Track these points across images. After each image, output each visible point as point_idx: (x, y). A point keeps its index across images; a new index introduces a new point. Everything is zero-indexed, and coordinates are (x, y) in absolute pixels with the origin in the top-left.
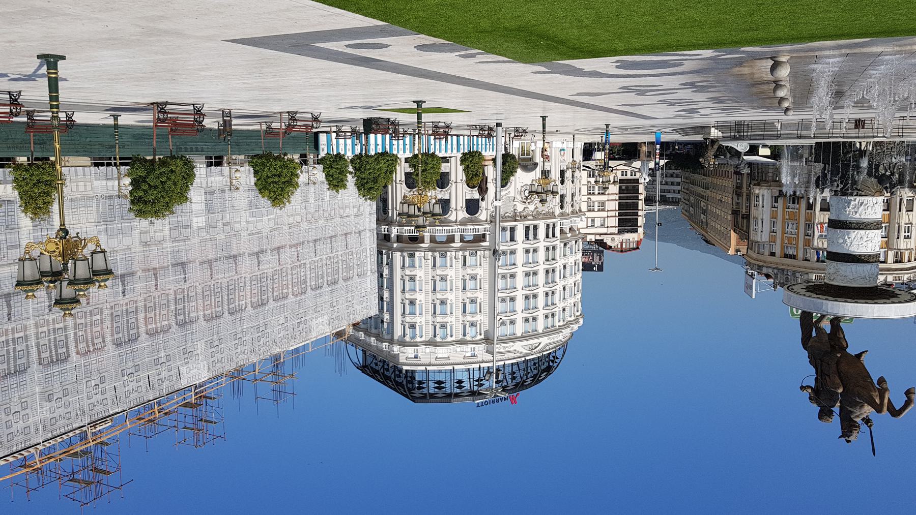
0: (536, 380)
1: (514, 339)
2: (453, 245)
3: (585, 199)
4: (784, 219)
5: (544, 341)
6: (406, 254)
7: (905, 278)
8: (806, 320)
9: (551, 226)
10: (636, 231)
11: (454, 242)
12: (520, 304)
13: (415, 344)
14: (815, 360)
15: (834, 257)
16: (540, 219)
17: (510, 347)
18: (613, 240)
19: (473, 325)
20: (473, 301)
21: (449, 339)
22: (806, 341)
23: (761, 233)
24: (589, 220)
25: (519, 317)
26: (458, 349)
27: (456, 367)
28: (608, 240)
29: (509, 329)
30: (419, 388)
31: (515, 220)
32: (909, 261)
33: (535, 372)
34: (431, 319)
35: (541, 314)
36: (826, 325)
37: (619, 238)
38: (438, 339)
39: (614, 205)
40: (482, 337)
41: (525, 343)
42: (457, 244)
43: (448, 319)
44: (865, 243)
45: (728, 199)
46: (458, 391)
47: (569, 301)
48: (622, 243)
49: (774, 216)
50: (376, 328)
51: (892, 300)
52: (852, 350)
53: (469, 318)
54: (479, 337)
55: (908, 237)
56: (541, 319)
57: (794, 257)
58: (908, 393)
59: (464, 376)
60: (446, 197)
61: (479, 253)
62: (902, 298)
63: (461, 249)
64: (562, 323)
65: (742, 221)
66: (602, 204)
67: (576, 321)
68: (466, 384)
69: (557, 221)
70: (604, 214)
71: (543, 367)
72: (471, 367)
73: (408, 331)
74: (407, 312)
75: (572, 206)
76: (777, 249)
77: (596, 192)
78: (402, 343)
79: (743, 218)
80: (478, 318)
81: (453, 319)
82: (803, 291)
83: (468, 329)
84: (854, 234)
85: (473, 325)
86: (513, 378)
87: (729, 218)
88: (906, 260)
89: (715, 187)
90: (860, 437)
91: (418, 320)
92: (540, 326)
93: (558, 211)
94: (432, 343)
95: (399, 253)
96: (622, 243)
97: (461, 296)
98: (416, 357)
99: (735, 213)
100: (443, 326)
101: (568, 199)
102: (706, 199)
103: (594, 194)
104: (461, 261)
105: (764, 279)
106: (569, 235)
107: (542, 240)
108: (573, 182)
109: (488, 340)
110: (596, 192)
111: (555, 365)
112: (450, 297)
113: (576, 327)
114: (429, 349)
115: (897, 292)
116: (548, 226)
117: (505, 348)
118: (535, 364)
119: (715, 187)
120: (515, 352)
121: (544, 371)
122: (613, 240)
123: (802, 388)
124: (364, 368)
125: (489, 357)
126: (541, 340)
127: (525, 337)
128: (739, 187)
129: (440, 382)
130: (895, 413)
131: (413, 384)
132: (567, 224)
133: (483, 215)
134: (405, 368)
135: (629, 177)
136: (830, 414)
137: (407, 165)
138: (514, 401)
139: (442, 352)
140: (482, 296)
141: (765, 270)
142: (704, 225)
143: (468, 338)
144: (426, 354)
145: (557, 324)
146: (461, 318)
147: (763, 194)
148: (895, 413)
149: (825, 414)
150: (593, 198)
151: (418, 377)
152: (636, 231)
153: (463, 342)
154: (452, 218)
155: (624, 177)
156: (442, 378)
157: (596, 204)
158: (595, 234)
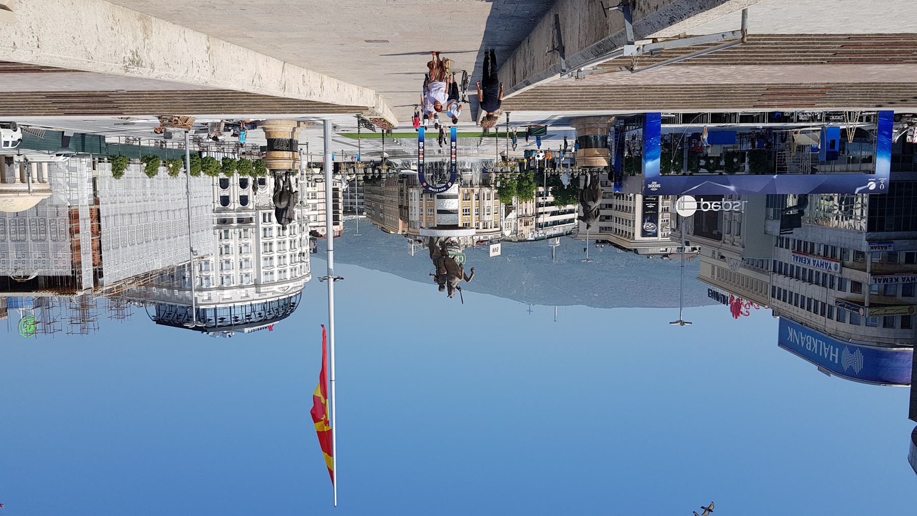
0: (285, 315)
1: (274, 284)
5: (291, 285)
13: (210, 290)
14: (436, 263)
15: (440, 212)
19: (247, 275)
20: (246, 260)
21: (232, 285)
23: (415, 215)
29: (269, 277)
34: (219, 273)
35: (288, 268)
38: (225, 285)
43: (232, 272)
44: (451, 204)
45: (396, 199)
49: (421, 205)
53: (245, 271)
56: (288, 272)
60: (227, 194)
63: (238, 227)
65: (404, 211)
67: (308, 275)
70: (316, 213)
73: (204, 281)
74: (203, 269)
76: (424, 225)
78: (200, 290)
80: (250, 271)
83: (244, 278)
84: (447, 200)
85: (247, 275)
87: (398, 210)
89: (388, 192)
90: (456, 293)
91: (212, 274)
92: (288, 275)
94: (221, 288)
97: (238, 257)
98: (209, 299)
99: (400, 207)
100: (228, 277)
102: (383, 202)
104: (238, 236)
105: (418, 244)
109: (257, 285)
112: (232, 258)
113: (308, 279)
114: (219, 293)
119: (388, 192)
120: (274, 292)
122: (323, 230)
124: (159, 321)
125: (257, 296)
129: (222, 319)
133: (250, 206)
134: (201, 307)
136: (444, 287)
138: (270, 328)
139: (227, 294)
140: (252, 257)
141: (418, 238)
142: (382, 220)
143: (244, 284)
144: (216, 295)
145: (299, 276)
146: (239, 272)
147: (415, 193)
149: (441, 288)
153: (241, 287)
154: (232, 208)
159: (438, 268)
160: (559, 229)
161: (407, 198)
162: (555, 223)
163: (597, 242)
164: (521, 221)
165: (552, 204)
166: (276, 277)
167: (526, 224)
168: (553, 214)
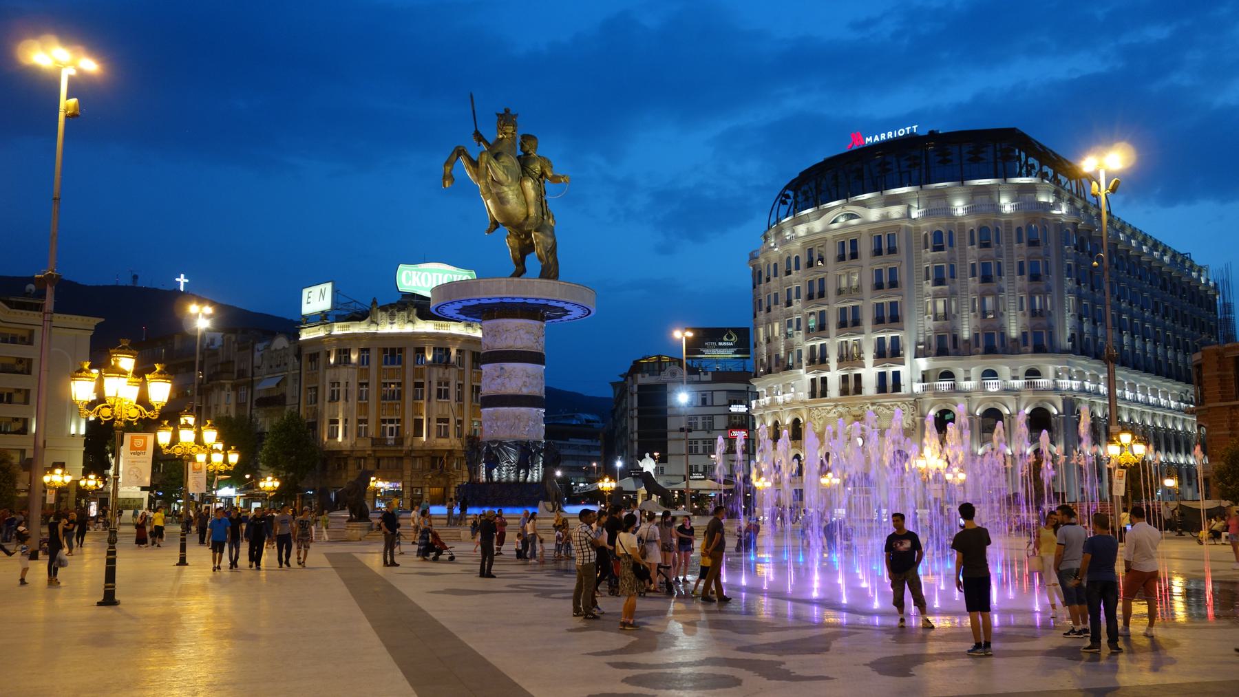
8: (550, 271)
10: (639, 386)
24: (709, 402)
51: (476, 302)
77: (700, 445)
152: (639, 386)
157: (700, 427)
167: (229, 362)
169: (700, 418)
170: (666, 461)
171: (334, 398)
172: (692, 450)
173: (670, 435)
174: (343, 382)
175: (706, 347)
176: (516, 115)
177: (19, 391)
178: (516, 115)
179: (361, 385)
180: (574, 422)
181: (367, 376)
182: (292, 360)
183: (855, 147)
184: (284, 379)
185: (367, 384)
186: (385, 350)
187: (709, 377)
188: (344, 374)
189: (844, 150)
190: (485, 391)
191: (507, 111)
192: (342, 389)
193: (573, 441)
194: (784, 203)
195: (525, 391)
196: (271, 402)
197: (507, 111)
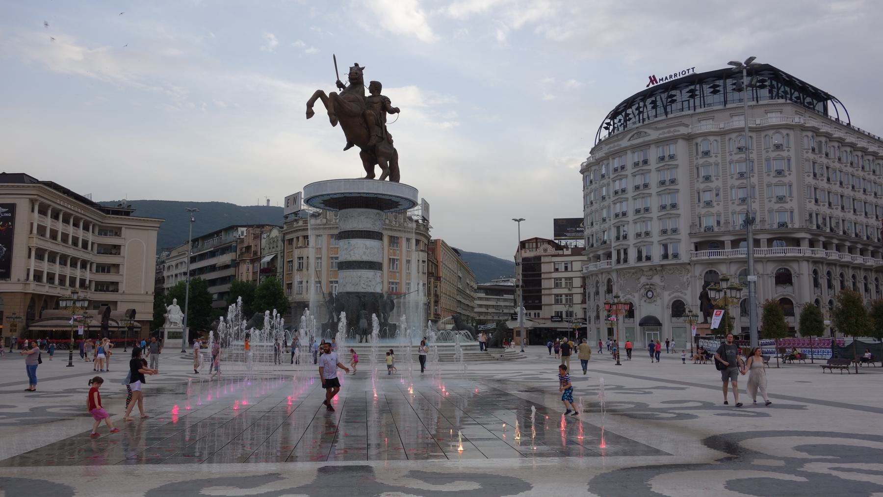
1: (658, 142)
2: (733, 238)
3: (574, 291)
4: (400, 273)
6: (790, 226)
7: (301, 223)
9: (622, 261)
10: (524, 259)
11: (732, 241)
12: (653, 179)
14: (388, 139)
16: (633, 268)
17: (664, 133)
18: (545, 250)
22: (393, 156)
24: (569, 269)
25: (653, 164)
26: (722, 126)
27: (721, 107)
28: (551, 250)
30: (763, 81)
31: (662, 266)
32: (298, 238)
33: (629, 111)
36: (378, 171)
37: (540, 252)
39: (545, 284)
40: (694, 141)
41: (647, 139)
42: (727, 239)
46: (717, 83)
47: (597, 185)
48: (537, 247)
49: (409, 274)
50: (821, 142)
51: (328, 197)
52: (356, 150)
54: (699, 140)
55: (299, 258)
57: (391, 237)
58: (310, 114)
59: (710, 99)
61: (702, 230)
62: (320, 200)
64: (605, 162)
66: (557, 285)
68: (707, 89)
69: (614, 266)
71: (620, 117)
72: (702, 110)
75: (598, 282)
77: (564, 297)
79: (432, 273)
81: (728, 159)
82: (402, 202)
86: (654, 102)
88: (301, 239)
93: (614, 276)
95: (797, 226)
96: (537, 247)
99: (438, 278)
101: (603, 289)
103: (566, 295)
106: (600, 252)
107: (631, 246)
108: (598, 306)
110: (564, 297)
111: (608, 121)
115: (322, 206)
116: (626, 261)
117: (669, 132)
118: (630, 119)
120: (657, 129)
121: (620, 113)
122: (545, 250)
123: (397, 110)
124: (822, 97)
126: (629, 143)
127: (647, 145)
128: (436, 302)
130: (320, 94)
131: (772, 86)
132: (603, 264)
133: (699, 271)
135: (532, 312)
137: (791, 325)
138: (653, 79)
148: (320, 94)
149: (376, 87)
150: (566, 291)
151: (765, 92)
155: (537, 311)
156: (736, 95)
157: (563, 286)
158: (563, 255)
159: (381, 123)
160: (209, 246)
161: (429, 289)
162: (213, 254)
163: (127, 214)
164: (255, 253)
165: (213, 282)
166: (653, 154)
167: (248, 248)
168: (213, 268)
169: (563, 281)
170: (540, 308)
171: (300, 269)
172: (558, 301)
173: (543, 292)
174: (305, 258)
175: (568, 232)
176: (363, 68)
177: (114, 265)
178: (363, 68)
179: (318, 258)
180: (509, 284)
181: (321, 254)
182: (280, 243)
183: (651, 86)
184: (275, 258)
185: (321, 258)
186: (332, 236)
187: (569, 252)
188: (304, 252)
189: (643, 88)
190: (341, 259)
191: (356, 65)
192: (305, 261)
193: (506, 296)
194: (606, 128)
195: (365, 258)
196: (269, 270)
197: (356, 65)
